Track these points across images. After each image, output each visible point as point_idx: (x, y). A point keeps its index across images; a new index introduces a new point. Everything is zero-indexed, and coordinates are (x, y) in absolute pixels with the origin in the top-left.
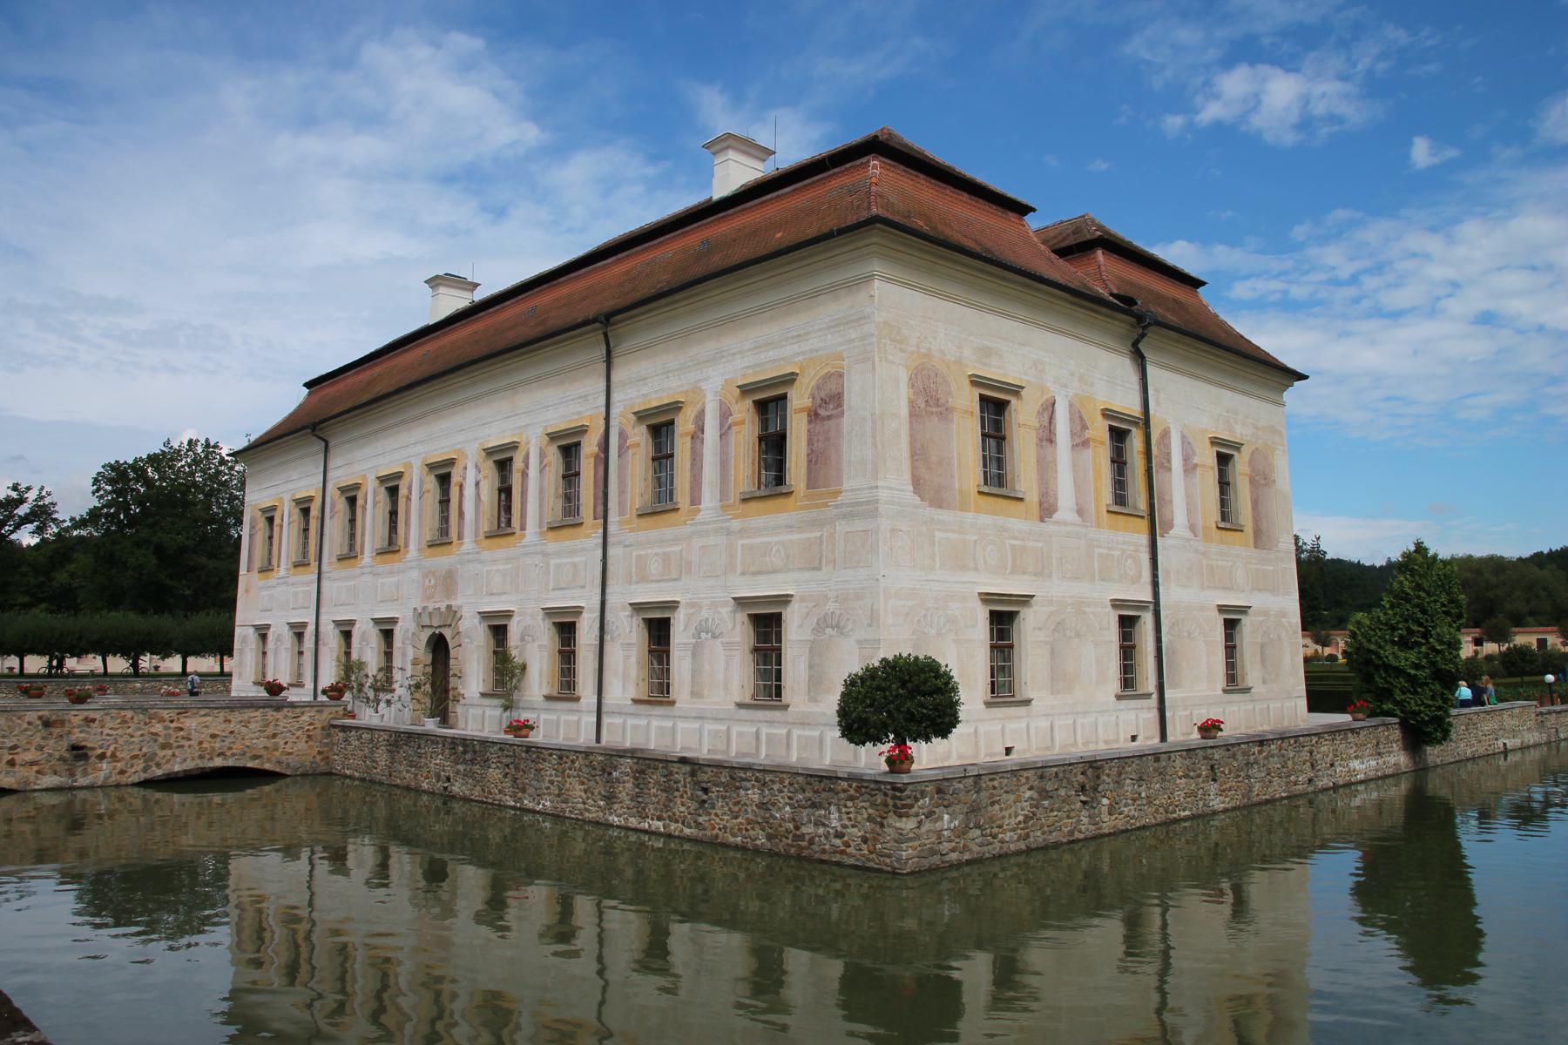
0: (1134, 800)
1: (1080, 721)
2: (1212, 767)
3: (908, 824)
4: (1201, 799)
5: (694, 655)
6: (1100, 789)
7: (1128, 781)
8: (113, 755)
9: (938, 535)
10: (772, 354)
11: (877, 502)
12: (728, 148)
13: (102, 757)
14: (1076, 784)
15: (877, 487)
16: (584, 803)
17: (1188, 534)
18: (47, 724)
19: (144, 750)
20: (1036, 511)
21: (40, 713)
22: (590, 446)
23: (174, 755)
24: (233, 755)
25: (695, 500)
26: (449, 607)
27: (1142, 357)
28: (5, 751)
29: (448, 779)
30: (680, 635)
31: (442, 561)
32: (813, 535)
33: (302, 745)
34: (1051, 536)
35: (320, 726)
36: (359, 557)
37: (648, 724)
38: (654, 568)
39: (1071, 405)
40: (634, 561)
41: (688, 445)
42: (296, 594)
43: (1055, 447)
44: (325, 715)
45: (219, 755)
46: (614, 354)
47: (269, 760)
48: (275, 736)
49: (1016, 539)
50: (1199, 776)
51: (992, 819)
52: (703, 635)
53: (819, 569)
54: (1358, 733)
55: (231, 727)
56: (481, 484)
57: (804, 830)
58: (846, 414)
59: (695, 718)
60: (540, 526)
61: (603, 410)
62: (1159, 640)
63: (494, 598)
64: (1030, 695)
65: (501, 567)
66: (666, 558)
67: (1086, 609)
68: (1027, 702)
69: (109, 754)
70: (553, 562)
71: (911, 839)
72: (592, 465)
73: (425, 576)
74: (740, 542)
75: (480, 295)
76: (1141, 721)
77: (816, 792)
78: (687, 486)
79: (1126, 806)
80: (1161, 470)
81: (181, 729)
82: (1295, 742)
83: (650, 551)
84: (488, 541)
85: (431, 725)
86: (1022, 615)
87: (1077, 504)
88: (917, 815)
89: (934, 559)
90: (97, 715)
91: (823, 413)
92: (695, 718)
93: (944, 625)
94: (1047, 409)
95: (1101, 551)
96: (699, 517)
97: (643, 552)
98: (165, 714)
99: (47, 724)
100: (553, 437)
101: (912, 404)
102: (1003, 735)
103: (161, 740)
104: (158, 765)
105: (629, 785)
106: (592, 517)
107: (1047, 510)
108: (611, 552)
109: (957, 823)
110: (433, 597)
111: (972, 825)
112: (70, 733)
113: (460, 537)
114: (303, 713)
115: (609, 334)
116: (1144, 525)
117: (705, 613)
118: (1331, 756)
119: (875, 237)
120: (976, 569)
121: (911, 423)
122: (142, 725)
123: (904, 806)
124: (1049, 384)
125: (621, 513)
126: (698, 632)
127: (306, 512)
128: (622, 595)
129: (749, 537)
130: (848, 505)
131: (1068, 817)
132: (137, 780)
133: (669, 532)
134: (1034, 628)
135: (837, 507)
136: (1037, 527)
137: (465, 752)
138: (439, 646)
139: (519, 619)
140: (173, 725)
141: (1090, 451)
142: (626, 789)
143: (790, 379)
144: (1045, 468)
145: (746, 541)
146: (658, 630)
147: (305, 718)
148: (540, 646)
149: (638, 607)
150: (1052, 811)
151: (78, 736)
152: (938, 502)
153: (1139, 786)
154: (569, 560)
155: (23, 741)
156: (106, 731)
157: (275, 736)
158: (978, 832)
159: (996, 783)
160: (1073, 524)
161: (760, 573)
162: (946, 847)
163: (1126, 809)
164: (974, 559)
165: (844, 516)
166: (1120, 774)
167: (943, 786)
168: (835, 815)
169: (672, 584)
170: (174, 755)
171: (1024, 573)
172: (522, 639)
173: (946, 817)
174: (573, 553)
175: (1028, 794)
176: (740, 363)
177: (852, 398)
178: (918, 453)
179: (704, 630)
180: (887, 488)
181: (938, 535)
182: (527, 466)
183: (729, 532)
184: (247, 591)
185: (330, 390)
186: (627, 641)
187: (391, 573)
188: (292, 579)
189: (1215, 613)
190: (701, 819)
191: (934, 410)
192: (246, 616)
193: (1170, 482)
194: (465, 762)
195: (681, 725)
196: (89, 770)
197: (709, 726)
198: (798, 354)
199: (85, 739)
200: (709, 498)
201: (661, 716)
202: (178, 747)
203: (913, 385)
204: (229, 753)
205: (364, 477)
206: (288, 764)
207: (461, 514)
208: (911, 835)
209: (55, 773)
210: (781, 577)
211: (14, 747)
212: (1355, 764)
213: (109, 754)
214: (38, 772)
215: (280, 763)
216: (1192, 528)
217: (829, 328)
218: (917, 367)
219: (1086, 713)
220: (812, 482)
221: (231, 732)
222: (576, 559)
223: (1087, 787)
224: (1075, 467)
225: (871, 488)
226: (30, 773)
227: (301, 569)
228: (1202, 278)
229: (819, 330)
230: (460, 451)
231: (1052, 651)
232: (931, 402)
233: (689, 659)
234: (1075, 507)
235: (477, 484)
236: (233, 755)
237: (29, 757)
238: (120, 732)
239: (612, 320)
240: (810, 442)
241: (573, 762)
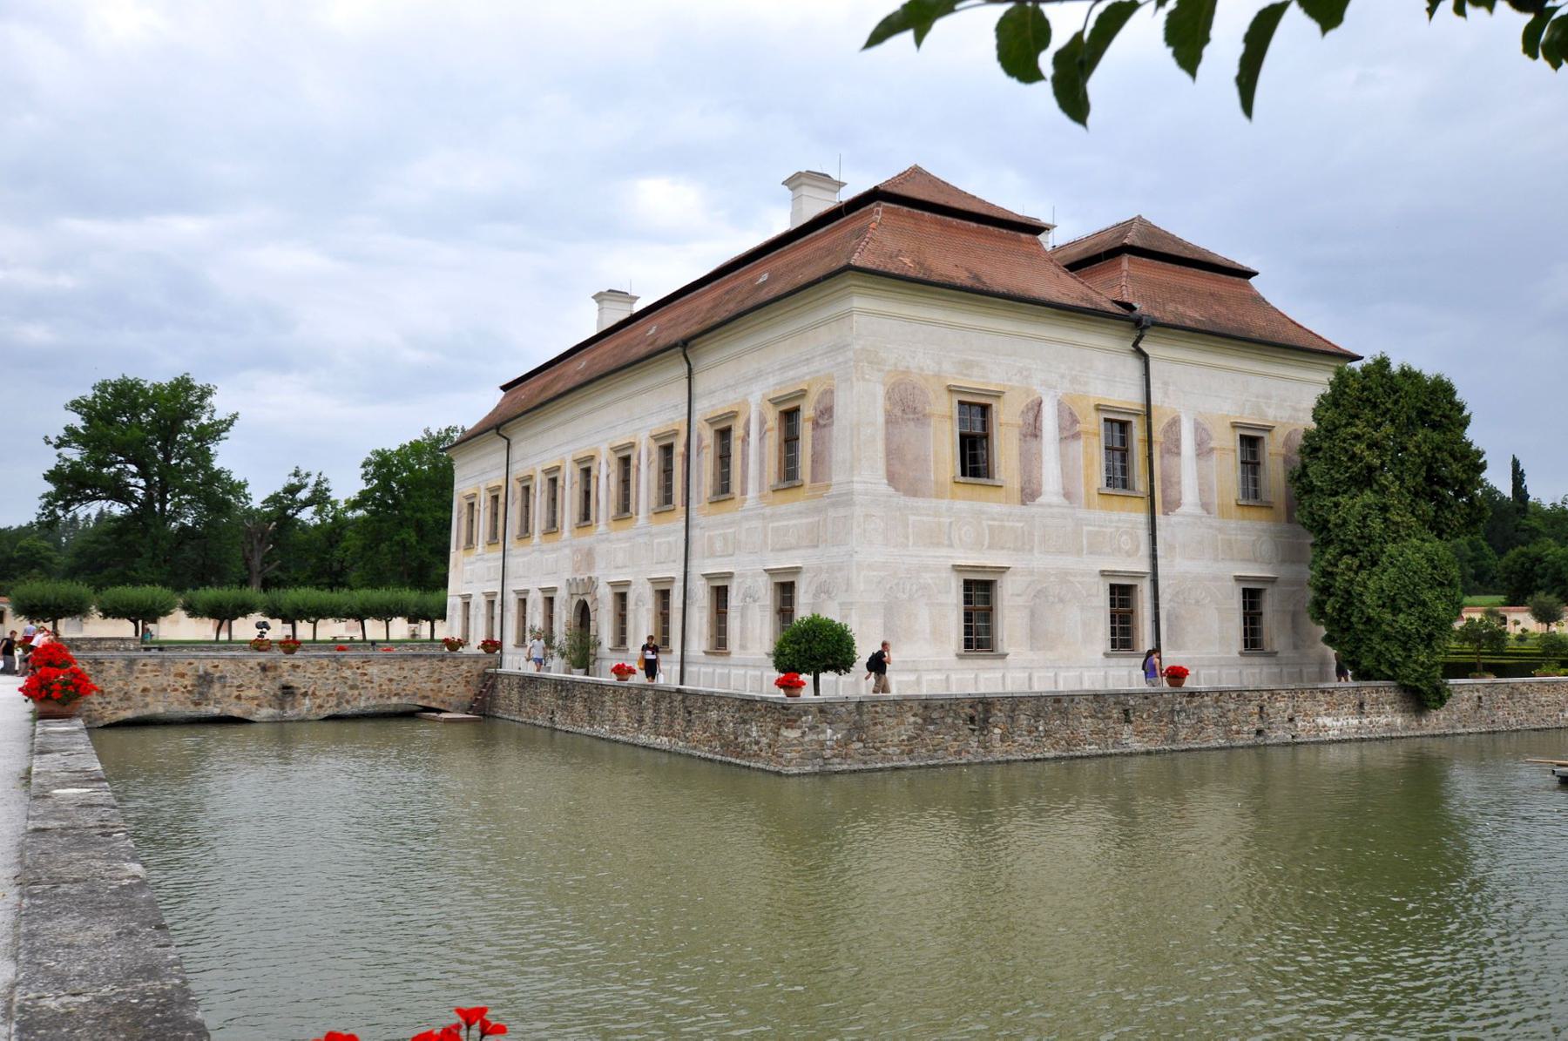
0: (1030, 732)
1: (1062, 674)
2: (1126, 712)
3: (792, 734)
4: (1111, 737)
5: (742, 616)
6: (991, 720)
7: (1022, 716)
8: (314, 694)
9: (912, 518)
10: (791, 374)
11: (852, 493)
12: (801, 185)
13: (305, 694)
14: (963, 715)
15: (852, 482)
16: (627, 726)
17: (1199, 511)
18: (264, 669)
19: (337, 690)
20: (1017, 495)
21: (259, 661)
22: (679, 449)
23: (360, 695)
24: (407, 695)
25: (744, 492)
26: (590, 578)
27: (1144, 358)
28: (234, 689)
29: (553, 712)
30: (734, 600)
31: (586, 540)
32: (810, 520)
33: (461, 689)
34: (1033, 517)
35: (475, 673)
38: (718, 545)
39: (1060, 403)
41: (740, 447)
42: (489, 568)
43: (1041, 443)
44: (480, 666)
45: (395, 695)
46: (695, 370)
47: (435, 700)
48: (439, 680)
49: (994, 519)
50: (1110, 718)
51: (874, 738)
53: (817, 546)
54: (1331, 694)
55: (405, 673)
57: (740, 740)
58: (835, 423)
60: (648, 512)
61: (686, 417)
62: (1156, 606)
63: (618, 571)
64: (1006, 651)
65: (623, 545)
67: (1071, 579)
68: (1003, 656)
69: (310, 693)
70: (656, 541)
71: (794, 745)
73: (574, 553)
74: (771, 525)
75: (638, 307)
76: (1135, 677)
77: (746, 712)
78: (739, 478)
79: (1019, 736)
80: (1167, 456)
81: (365, 674)
82: (1238, 696)
85: (578, 676)
86: (999, 582)
87: (1064, 489)
88: (800, 727)
89: (907, 538)
90: (301, 663)
91: (822, 422)
93: (917, 591)
94: (1032, 408)
95: (1090, 528)
96: (746, 505)
98: (353, 662)
99: (264, 669)
100: (656, 438)
101: (888, 415)
102: (976, 682)
103: (350, 682)
104: (348, 702)
105: (651, 711)
107: (1029, 494)
108: (693, 533)
109: (839, 736)
110: (579, 570)
111: (854, 739)
112: (281, 676)
113: (597, 521)
114: (462, 663)
115: (689, 356)
116: (1143, 505)
117: (749, 582)
118: (1290, 711)
119: (850, 280)
120: (951, 546)
121: (887, 429)
122: (334, 671)
123: (789, 720)
124: (1035, 387)
125: (699, 502)
127: (496, 498)
131: (955, 740)
132: (331, 713)
133: (727, 517)
134: (1012, 595)
135: (828, 497)
136: (1018, 509)
137: (561, 691)
138: (584, 613)
140: (359, 671)
141: (1081, 442)
142: (649, 714)
143: (802, 394)
144: (1030, 462)
145: (776, 524)
146: (720, 595)
147: (464, 667)
149: (708, 577)
150: (938, 734)
151: (287, 678)
152: (913, 490)
153: (1036, 722)
155: (246, 681)
156: (308, 675)
157: (439, 680)
158: (861, 745)
159: (878, 709)
160: (1058, 506)
161: (782, 550)
162: (828, 753)
163: (1021, 739)
164: (950, 538)
165: (834, 505)
166: (1013, 711)
167: (825, 711)
168: (754, 729)
170: (360, 695)
171: (1002, 548)
172: (636, 604)
173: (829, 731)
175: (912, 719)
176: (772, 380)
177: (838, 411)
178: (893, 454)
179: (749, 596)
180: (861, 482)
181: (912, 518)
182: (639, 463)
184: (456, 566)
185: (522, 393)
187: (553, 550)
188: (486, 556)
189: (1232, 583)
190: (688, 734)
191: (912, 416)
192: (457, 585)
193: (1179, 466)
194: (562, 698)
195: (734, 671)
196: (296, 704)
197: (751, 672)
198: (807, 374)
199: (292, 681)
200: (752, 490)
202: (363, 688)
203: (890, 398)
204: (402, 694)
205: (534, 469)
206: (450, 704)
208: (795, 742)
209: (270, 706)
211: (240, 686)
212: (1328, 721)
213: (310, 693)
214: (258, 705)
215: (443, 702)
216: (1205, 506)
218: (894, 383)
219: (1068, 668)
220: (814, 479)
221: (405, 677)
223: (976, 718)
224: (1063, 457)
225: (848, 483)
226: (252, 706)
227: (493, 546)
228: (1254, 268)
229: (820, 355)
230: (596, 449)
231: (1032, 615)
232: (907, 410)
233: (739, 620)
234: (1061, 491)
235: (608, 476)
236: (407, 695)
237: (251, 693)
238: (319, 675)
239: (690, 344)
240: (813, 446)
241: (621, 694)
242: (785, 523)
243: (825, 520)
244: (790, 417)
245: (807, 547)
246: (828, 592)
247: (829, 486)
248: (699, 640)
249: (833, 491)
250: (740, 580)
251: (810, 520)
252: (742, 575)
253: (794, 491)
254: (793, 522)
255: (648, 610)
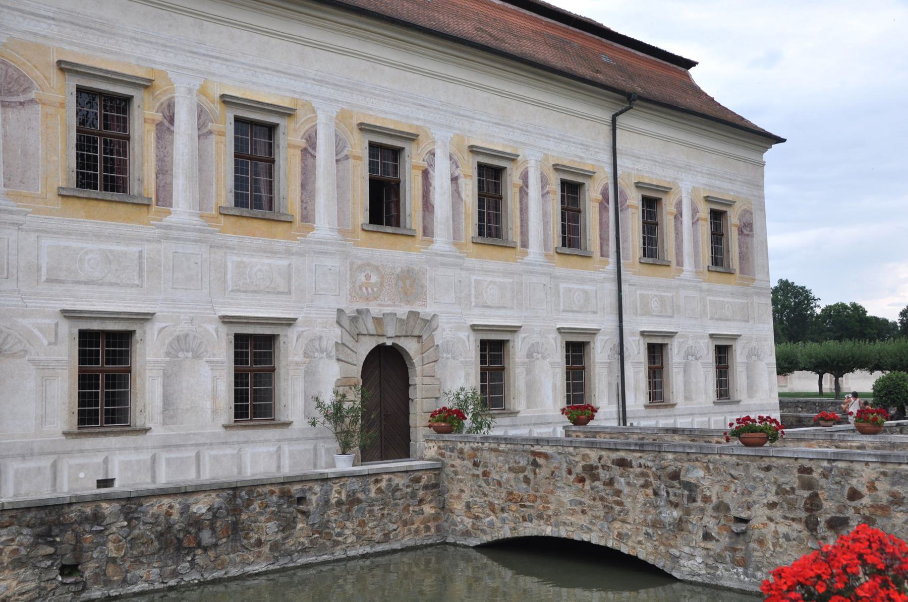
5: (685, 371)
25: (680, 263)
26: (414, 314)
36: (154, 208)
37: (692, 420)
38: (654, 305)
40: (638, 298)
52: (690, 357)
53: (747, 321)
56: (461, 181)
59: (688, 415)
63: (488, 312)
65: (497, 280)
66: (662, 301)
72: (597, 209)
74: (708, 298)
83: (650, 293)
84: (476, 247)
92: (688, 415)
97: (645, 292)
106: (599, 254)
117: (691, 342)
126: (687, 355)
128: (635, 324)
129: (713, 296)
130: (758, 288)
139: (523, 335)
145: (712, 298)
148: (552, 364)
154: (580, 287)
161: (720, 319)
169: (669, 319)
172: (530, 355)
174: (582, 281)
179: (690, 354)
182: (526, 184)
183: (701, 290)
186: (636, 361)
201: (665, 416)
207: (427, 206)
210: (732, 324)
217: (708, 174)
222: (587, 287)
233: (682, 374)
235: (454, 179)
240: (740, 246)
242: (721, 299)
243: (752, 303)
244: (717, 216)
245: (741, 321)
246: (757, 355)
247: (754, 280)
248: (637, 397)
249: (756, 284)
250: (682, 340)
251: (740, 301)
252: (683, 336)
253: (728, 276)
254: (726, 300)
255: (768, 364)
